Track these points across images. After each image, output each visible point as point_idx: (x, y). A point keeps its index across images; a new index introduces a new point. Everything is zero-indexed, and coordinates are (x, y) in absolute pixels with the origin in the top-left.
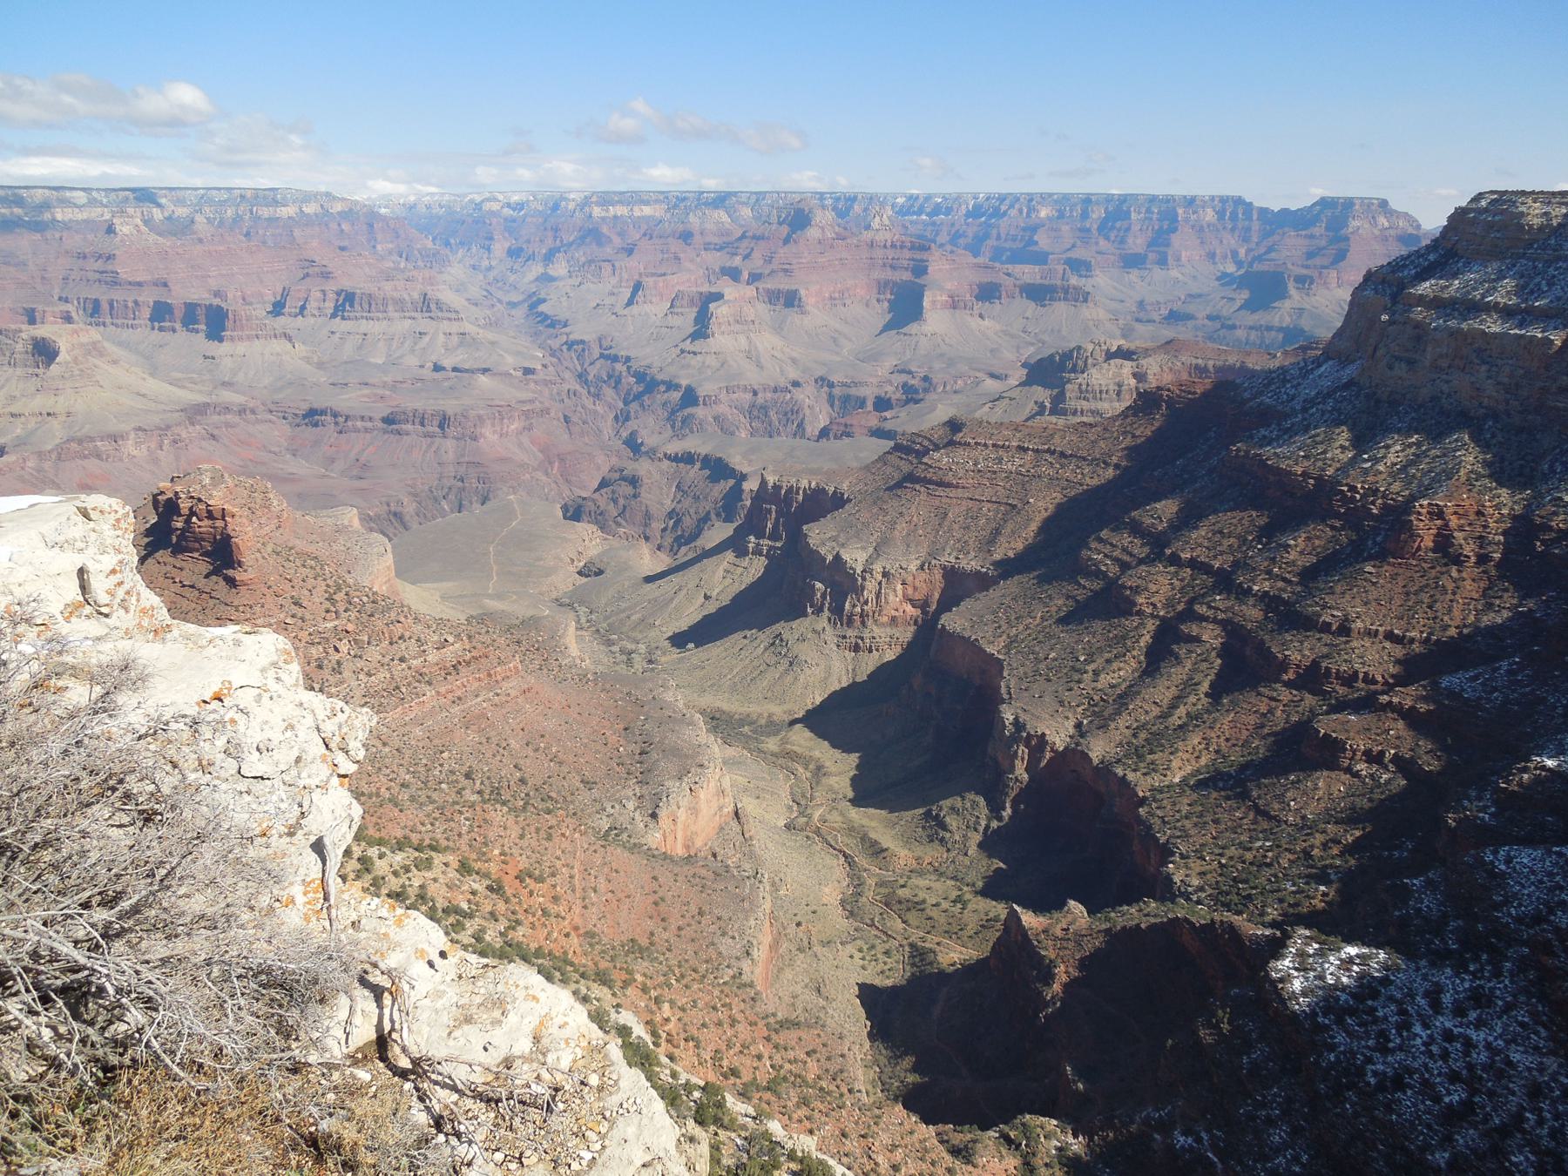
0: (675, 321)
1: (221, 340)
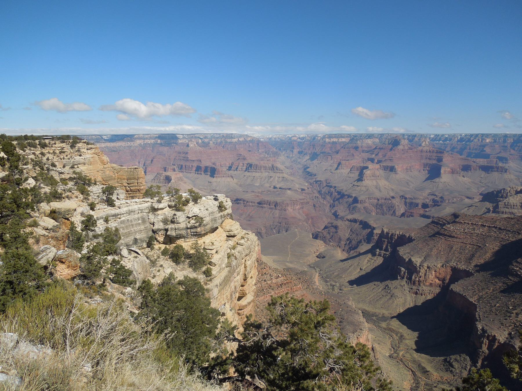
0: (352, 175)
1: (214, 177)
